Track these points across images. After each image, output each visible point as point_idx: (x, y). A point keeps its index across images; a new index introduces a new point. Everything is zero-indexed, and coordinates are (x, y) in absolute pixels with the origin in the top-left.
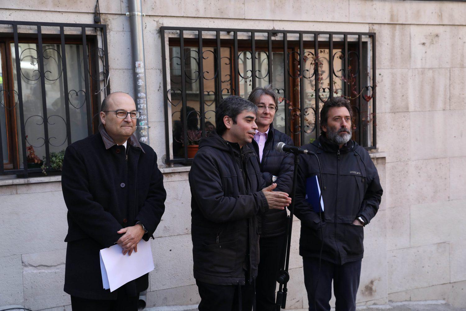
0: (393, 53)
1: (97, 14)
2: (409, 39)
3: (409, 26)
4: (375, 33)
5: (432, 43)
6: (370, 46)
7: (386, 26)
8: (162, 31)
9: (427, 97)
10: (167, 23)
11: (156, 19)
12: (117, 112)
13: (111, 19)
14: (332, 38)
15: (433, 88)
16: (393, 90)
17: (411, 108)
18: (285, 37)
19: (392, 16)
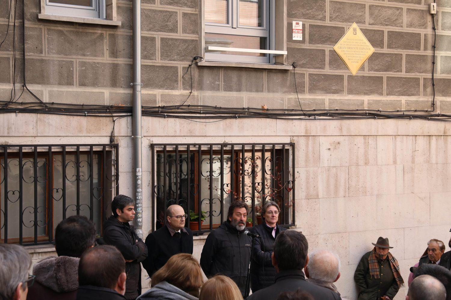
1: (112, 138)
2: (318, 146)
3: (318, 137)
4: (294, 143)
6: (291, 152)
7: (303, 137)
8: (152, 146)
10: (156, 141)
11: (149, 138)
12: (177, 217)
13: (120, 139)
14: (265, 147)
15: (336, 181)
16: (308, 183)
18: (232, 147)
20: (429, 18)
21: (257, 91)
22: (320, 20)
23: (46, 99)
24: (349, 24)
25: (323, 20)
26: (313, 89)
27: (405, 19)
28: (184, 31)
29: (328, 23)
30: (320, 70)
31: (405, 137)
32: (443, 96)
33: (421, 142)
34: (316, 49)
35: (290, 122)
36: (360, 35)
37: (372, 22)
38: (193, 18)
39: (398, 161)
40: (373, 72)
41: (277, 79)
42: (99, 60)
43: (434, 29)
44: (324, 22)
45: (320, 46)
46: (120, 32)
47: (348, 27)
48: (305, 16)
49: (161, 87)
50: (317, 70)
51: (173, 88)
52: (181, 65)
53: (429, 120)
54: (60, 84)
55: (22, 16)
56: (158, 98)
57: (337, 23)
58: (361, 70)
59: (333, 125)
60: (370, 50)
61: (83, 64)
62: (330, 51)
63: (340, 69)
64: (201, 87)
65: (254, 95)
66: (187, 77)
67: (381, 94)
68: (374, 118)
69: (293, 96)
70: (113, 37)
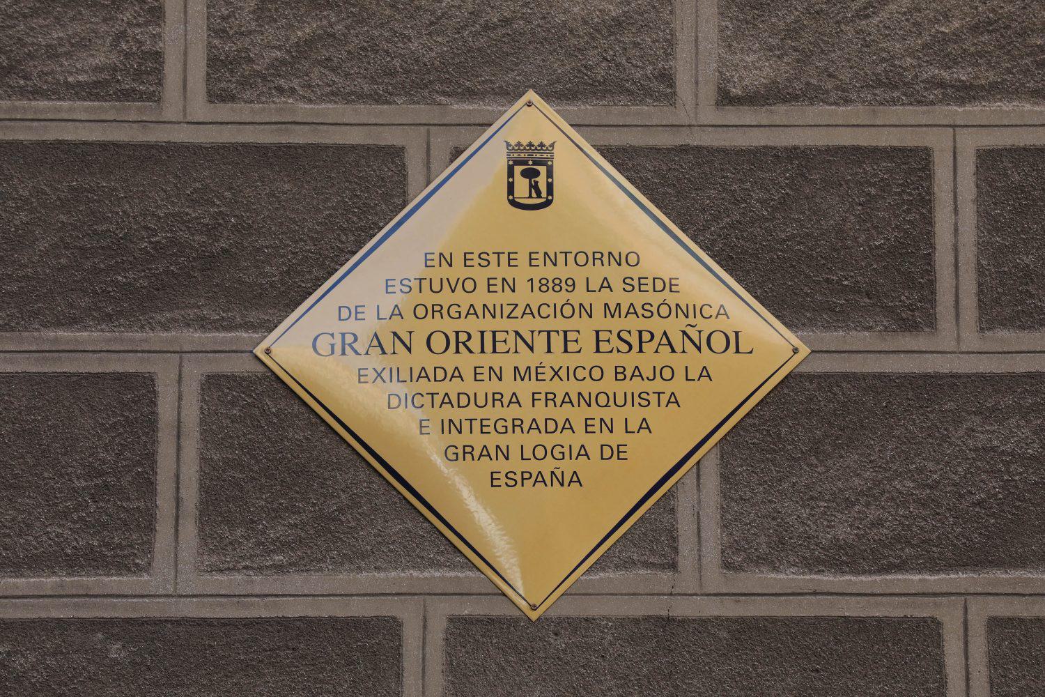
22: (91, 91)
24: (460, 109)
25: (126, 95)
30: (88, 580)
34: (28, 378)
40: (789, 577)
44: (133, 110)
47: (441, 142)
50: (48, 582)
57: (304, 110)
58: (628, 564)
62: (213, 382)
63: (356, 558)
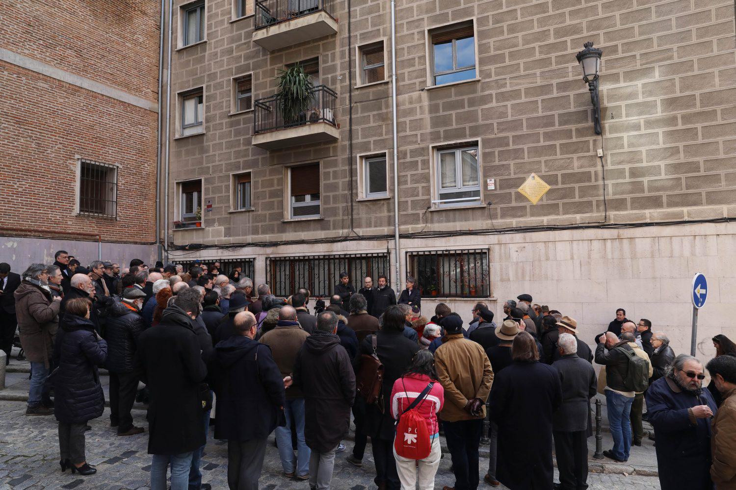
0: (500, 255)
1: (388, 249)
5: (522, 250)
9: (520, 274)
10: (409, 250)
17: (511, 279)
19: (499, 241)
20: (599, 160)
21: (466, 221)
23: (361, 234)
26: (503, 216)
27: (576, 164)
28: (423, 195)
29: (513, 176)
31: (580, 241)
32: (616, 211)
33: (596, 245)
35: (487, 236)
36: (538, 179)
37: (547, 170)
38: (427, 188)
39: (575, 257)
41: (479, 213)
42: (382, 215)
43: (603, 166)
45: (508, 191)
46: (391, 201)
48: (495, 175)
49: (412, 224)
51: (418, 224)
52: (421, 212)
53: (602, 228)
54: (367, 227)
55: (352, 201)
56: (410, 229)
59: (518, 237)
60: (548, 187)
61: (376, 217)
64: (432, 222)
65: (463, 223)
66: (424, 217)
67: (558, 214)
68: (551, 230)
69: (489, 222)
70: (388, 204)
